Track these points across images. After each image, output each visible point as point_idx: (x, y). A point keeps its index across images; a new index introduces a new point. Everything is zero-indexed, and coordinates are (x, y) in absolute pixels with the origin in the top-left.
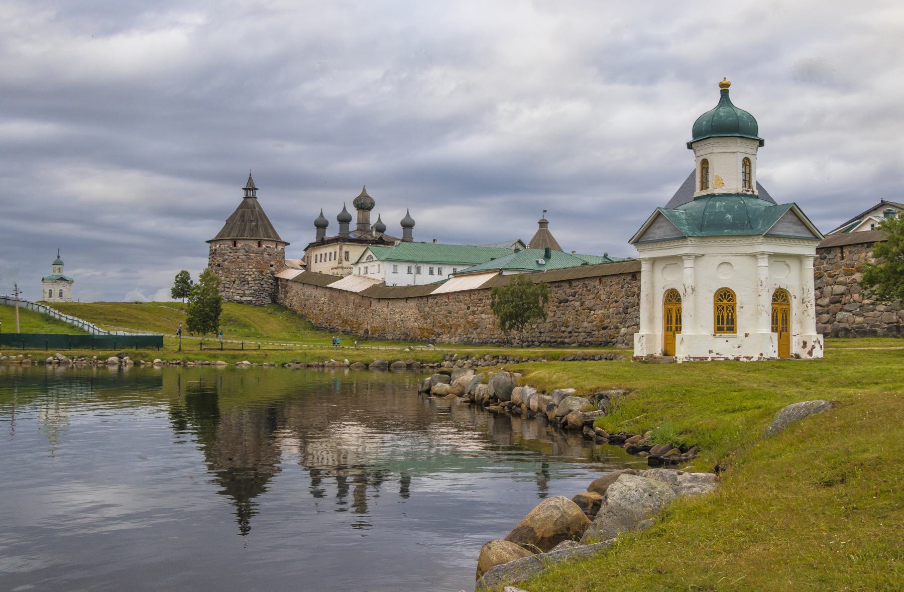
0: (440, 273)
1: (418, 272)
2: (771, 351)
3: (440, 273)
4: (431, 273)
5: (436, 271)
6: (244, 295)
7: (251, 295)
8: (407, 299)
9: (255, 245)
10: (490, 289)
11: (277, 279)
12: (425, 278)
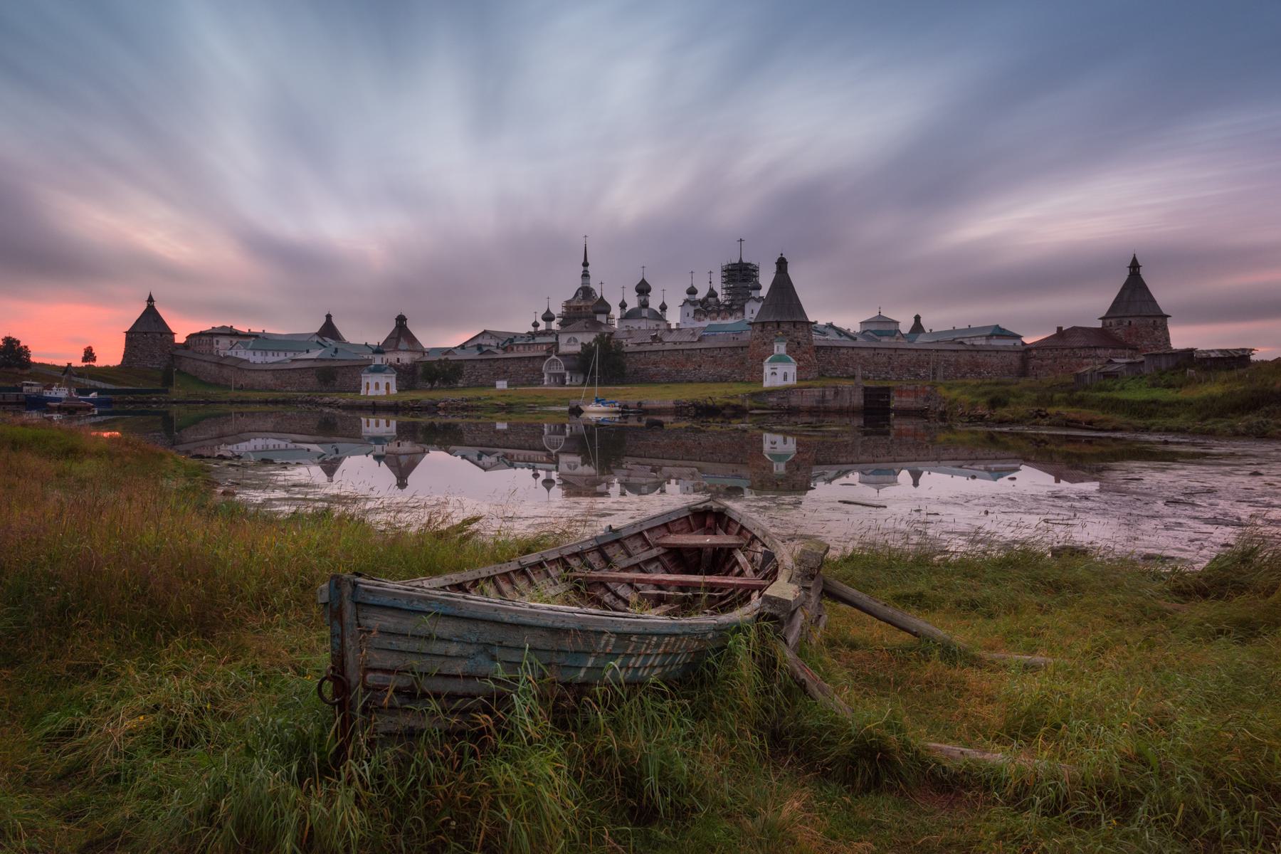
0: (278, 355)
1: (267, 355)
2: (385, 393)
3: (278, 355)
4: (273, 355)
5: (276, 355)
6: (154, 364)
7: (159, 364)
8: (266, 370)
9: (159, 336)
10: (313, 368)
11: (173, 355)
12: (271, 358)
